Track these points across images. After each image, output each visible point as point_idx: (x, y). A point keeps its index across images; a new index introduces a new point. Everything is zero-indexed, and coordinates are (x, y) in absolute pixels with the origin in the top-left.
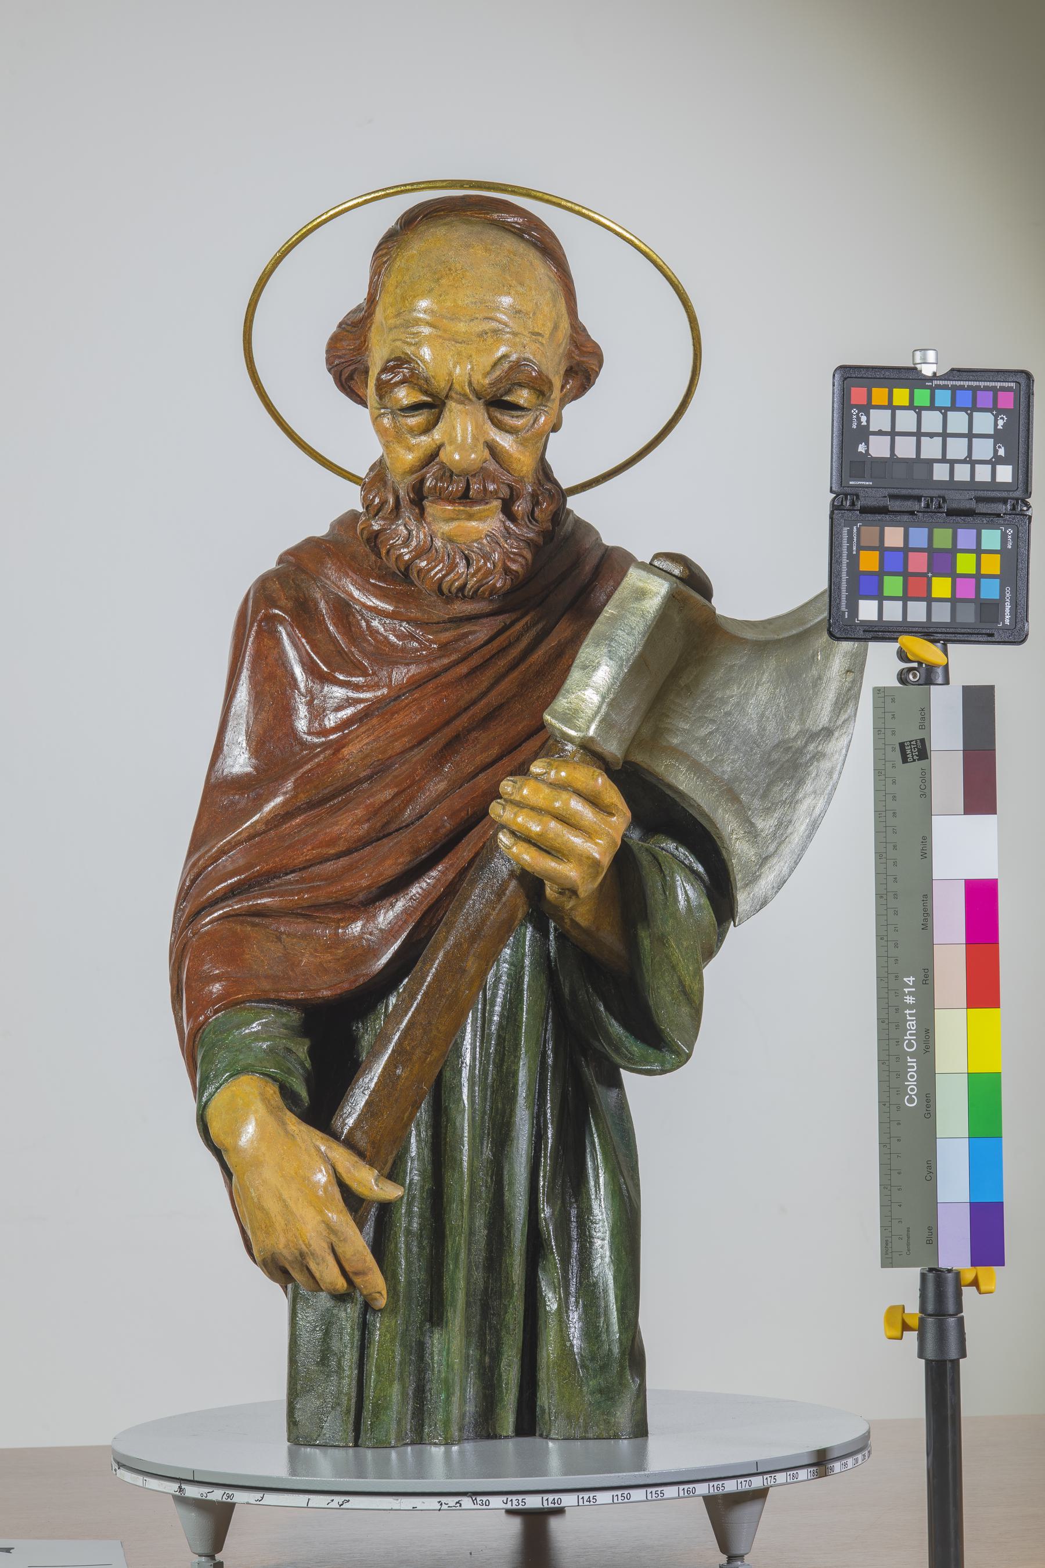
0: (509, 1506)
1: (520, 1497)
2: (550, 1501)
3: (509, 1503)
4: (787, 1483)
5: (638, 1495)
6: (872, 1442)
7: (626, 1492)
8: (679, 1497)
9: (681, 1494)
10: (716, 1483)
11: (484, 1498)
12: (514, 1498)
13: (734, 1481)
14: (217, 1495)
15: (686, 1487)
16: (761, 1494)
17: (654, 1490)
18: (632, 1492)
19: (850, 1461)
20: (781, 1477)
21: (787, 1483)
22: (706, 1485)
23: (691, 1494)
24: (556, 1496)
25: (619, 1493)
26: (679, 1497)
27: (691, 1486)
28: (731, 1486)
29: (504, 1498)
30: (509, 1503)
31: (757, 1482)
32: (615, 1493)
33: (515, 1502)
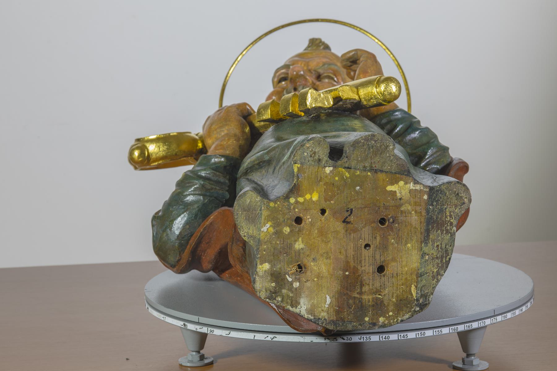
0: (362, 340)
2: (384, 336)
3: (362, 339)
9: (451, 331)
11: (349, 337)
15: (453, 327)
17: (437, 330)
21: (502, 321)
25: (419, 332)
27: (456, 327)
28: (475, 325)
29: (360, 337)
30: (362, 339)
32: (417, 333)
33: (365, 339)
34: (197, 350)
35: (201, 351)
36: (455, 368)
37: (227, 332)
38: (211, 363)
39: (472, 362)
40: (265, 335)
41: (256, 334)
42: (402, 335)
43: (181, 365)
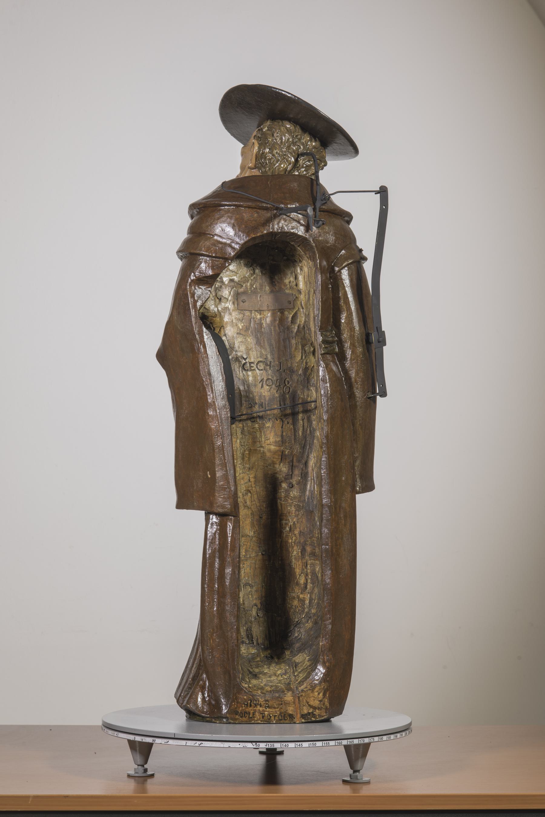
0: (267, 747)
1: (272, 744)
2: (284, 744)
4: (378, 741)
5: (319, 744)
6: (412, 726)
7: (314, 742)
8: (335, 745)
10: (350, 740)
12: (270, 744)
13: (357, 740)
14: (149, 740)
15: (338, 741)
16: (367, 746)
18: (317, 742)
19: (404, 734)
20: (376, 739)
21: (378, 741)
22: (346, 741)
23: (340, 744)
24: (286, 744)
26: (335, 745)
28: (356, 741)
29: (266, 744)
31: (367, 740)
32: (310, 743)
34: (141, 764)
35: (146, 766)
36: (344, 782)
37: (166, 740)
38: (152, 776)
39: (357, 776)
40: (195, 742)
41: (188, 742)
42: (298, 743)
43: (129, 776)
